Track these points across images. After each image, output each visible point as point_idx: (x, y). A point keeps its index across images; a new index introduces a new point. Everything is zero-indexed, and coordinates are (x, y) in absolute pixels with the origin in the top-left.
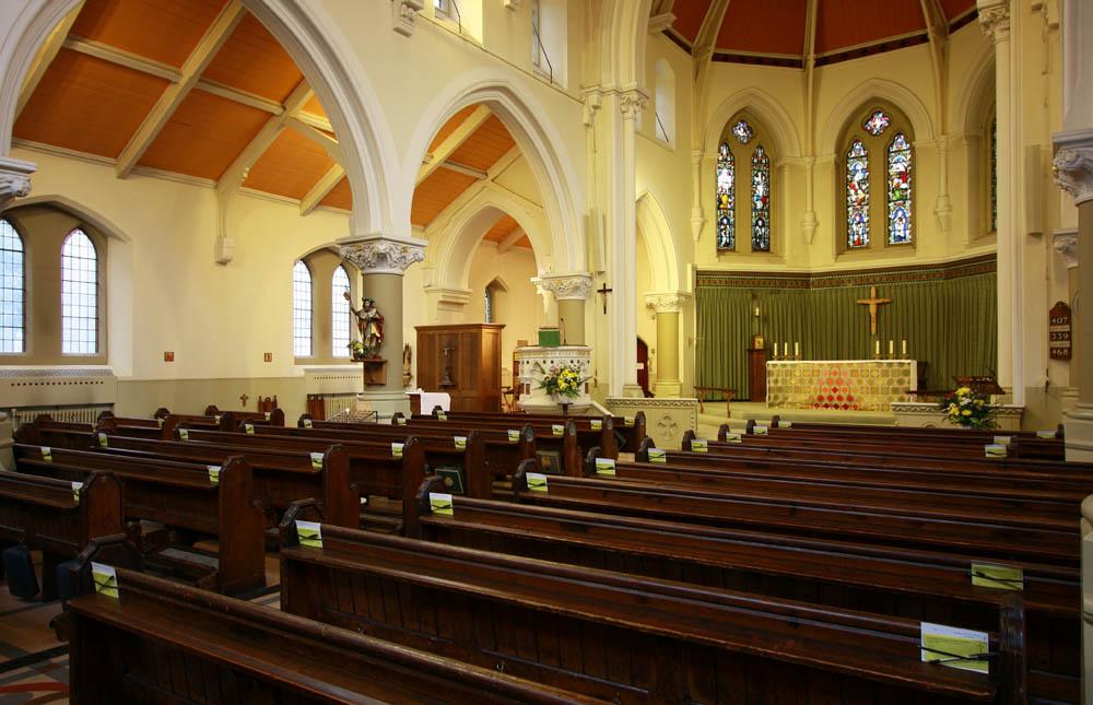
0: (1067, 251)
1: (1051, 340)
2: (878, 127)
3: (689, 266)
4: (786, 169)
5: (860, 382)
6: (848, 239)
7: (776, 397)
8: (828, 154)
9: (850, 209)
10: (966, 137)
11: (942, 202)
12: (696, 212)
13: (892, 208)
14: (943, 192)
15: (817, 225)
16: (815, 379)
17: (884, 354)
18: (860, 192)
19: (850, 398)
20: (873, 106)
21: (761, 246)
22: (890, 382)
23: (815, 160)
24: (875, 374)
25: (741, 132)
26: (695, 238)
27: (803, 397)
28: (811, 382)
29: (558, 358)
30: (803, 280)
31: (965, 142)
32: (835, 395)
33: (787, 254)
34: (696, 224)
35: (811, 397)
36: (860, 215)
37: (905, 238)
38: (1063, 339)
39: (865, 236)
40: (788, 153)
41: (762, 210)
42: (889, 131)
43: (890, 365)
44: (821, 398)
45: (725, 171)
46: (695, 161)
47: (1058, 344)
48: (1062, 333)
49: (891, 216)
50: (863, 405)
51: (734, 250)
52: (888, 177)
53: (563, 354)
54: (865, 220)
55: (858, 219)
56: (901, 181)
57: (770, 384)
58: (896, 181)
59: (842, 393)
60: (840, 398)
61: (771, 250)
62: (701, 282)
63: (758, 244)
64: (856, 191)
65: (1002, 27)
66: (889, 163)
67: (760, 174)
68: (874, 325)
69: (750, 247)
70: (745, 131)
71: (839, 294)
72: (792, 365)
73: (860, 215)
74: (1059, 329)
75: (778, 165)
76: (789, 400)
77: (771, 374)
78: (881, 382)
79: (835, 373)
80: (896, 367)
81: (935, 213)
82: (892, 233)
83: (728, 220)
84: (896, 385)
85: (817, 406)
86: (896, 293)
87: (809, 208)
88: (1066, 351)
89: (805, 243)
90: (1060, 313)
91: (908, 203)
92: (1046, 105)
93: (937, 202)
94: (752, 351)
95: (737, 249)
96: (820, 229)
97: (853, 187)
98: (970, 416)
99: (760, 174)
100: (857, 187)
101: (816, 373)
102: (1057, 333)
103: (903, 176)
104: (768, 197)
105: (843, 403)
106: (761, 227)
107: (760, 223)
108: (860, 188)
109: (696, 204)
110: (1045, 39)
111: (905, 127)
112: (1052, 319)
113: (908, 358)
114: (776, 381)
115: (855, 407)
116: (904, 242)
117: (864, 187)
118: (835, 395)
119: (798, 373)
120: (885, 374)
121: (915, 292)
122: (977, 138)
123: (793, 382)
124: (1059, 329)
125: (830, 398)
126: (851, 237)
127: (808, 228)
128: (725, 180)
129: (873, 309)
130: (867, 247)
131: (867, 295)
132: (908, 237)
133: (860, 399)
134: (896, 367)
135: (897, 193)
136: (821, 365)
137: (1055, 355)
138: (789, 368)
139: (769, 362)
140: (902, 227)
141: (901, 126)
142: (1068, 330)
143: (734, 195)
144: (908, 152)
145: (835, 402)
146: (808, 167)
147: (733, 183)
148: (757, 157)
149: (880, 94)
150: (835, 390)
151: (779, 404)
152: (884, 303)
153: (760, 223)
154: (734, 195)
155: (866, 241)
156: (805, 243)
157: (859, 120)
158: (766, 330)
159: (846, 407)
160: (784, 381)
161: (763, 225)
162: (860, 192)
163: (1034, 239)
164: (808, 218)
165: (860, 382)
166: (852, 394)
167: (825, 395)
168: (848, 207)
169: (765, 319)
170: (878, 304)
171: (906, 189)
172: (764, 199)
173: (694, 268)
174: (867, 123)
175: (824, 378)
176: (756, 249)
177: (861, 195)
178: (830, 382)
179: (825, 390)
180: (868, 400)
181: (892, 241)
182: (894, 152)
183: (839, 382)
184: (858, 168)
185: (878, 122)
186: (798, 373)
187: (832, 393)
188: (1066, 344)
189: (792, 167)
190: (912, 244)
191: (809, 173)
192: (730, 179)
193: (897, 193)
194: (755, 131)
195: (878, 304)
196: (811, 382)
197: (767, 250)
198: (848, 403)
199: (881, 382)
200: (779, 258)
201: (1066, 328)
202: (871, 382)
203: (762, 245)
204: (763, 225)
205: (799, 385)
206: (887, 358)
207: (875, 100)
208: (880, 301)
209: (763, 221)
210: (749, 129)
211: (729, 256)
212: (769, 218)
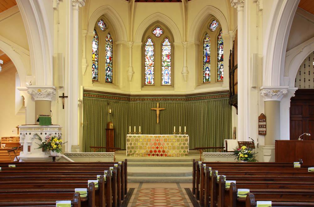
0: (266, 95)
1: (259, 128)
2: (158, 33)
3: (82, 87)
4: (121, 46)
5: (168, 144)
6: (145, 81)
7: (131, 151)
8: (138, 42)
10: (195, 44)
11: (185, 69)
12: (84, 61)
14: (185, 65)
15: (134, 73)
16: (148, 143)
17: (177, 133)
18: (150, 60)
19: (164, 151)
20: (157, 24)
21: (109, 81)
22: (180, 144)
23: (133, 44)
24: (174, 140)
25: (101, 26)
26: (83, 73)
27: (143, 151)
28: (147, 144)
29: (46, 133)
30: (127, 98)
31: (194, 46)
32: (157, 150)
33: (121, 84)
34: (84, 67)
35: (147, 151)
36: (150, 71)
37: (168, 82)
38: (263, 127)
39: (152, 80)
40: (122, 39)
41: (109, 63)
42: (163, 36)
43: (180, 137)
44: (151, 152)
45: (94, 42)
46: (84, 35)
47: (261, 129)
48: (263, 125)
49: (163, 73)
50: (169, 154)
51: (97, 81)
52: (162, 55)
53: (51, 130)
55: (149, 72)
56: (167, 58)
57: (128, 145)
59: (160, 149)
60: (159, 151)
61: (113, 82)
62: (85, 95)
63: (107, 79)
64: (149, 60)
65: (241, 6)
67: (109, 46)
68: (158, 119)
69: (104, 80)
70: (103, 25)
71: (143, 105)
72: (138, 136)
73: (150, 71)
74: (262, 123)
75: (117, 43)
76: (137, 152)
77: (128, 140)
78: (176, 144)
79: (157, 140)
80: (182, 138)
81: (182, 74)
82: (163, 80)
83: (95, 66)
84: (182, 145)
85: (149, 155)
86: (166, 106)
87: (130, 65)
88: (264, 132)
89: (128, 81)
90: (262, 118)
91: (170, 68)
92: (257, 39)
93: (183, 69)
94: (108, 129)
95: (99, 81)
96: (135, 75)
97: (148, 58)
98: (247, 157)
99: (109, 46)
100: (149, 58)
101: (149, 140)
102: (261, 125)
103: (168, 56)
104: (112, 57)
105: (161, 154)
106: (109, 71)
107: (108, 69)
109: (84, 56)
110: (257, 15)
111: (170, 36)
112: (259, 120)
113: (187, 134)
114: (131, 144)
115: (166, 155)
116: (168, 84)
118: (157, 150)
119: (141, 140)
120: (178, 140)
121: (174, 106)
122: (198, 45)
123: (139, 144)
124: (262, 123)
125: (155, 151)
126: (146, 80)
127: (130, 74)
128: (95, 47)
129: (158, 112)
130: (154, 85)
131: (155, 106)
132: (170, 82)
133: (168, 152)
134: (182, 138)
135: (165, 63)
136: (151, 136)
137: (260, 133)
138: (137, 138)
139: (127, 135)
140: (167, 78)
141: (168, 34)
142: (265, 124)
143: (98, 55)
145: (157, 153)
146: (130, 46)
147: (98, 49)
148: (108, 38)
149: (161, 20)
150: (157, 148)
151: (132, 155)
152: (161, 110)
153: (108, 69)
154: (98, 55)
155: (153, 82)
156: (128, 81)
157: (152, 28)
158: (113, 120)
159: (162, 155)
160: (135, 144)
161: (110, 71)
162: (150, 60)
163: (253, 89)
164: (130, 69)
165: (168, 144)
166: (165, 149)
167: (153, 150)
168: (145, 66)
169: (112, 114)
170: (160, 110)
171: (169, 62)
172: (110, 58)
173: (83, 88)
175: (153, 142)
176: (107, 82)
177: (151, 62)
178: (155, 144)
179: (153, 148)
180: (171, 152)
181: (163, 84)
183: (159, 144)
184: (149, 50)
185: (158, 32)
186: (141, 140)
187: (156, 149)
188: (264, 129)
189: (124, 45)
190: (172, 85)
191: (130, 49)
192: (96, 47)
193: (165, 63)
194: (107, 27)
195: (160, 110)
196: (147, 144)
197: (111, 82)
198: (163, 154)
199: (176, 144)
200: (117, 87)
201: (264, 123)
202: (172, 144)
203: (109, 80)
204: (110, 71)
205: (141, 146)
206: (178, 134)
207: (158, 22)
208: (161, 109)
209: (110, 69)
210: (104, 24)
211: (96, 83)
212: (112, 67)
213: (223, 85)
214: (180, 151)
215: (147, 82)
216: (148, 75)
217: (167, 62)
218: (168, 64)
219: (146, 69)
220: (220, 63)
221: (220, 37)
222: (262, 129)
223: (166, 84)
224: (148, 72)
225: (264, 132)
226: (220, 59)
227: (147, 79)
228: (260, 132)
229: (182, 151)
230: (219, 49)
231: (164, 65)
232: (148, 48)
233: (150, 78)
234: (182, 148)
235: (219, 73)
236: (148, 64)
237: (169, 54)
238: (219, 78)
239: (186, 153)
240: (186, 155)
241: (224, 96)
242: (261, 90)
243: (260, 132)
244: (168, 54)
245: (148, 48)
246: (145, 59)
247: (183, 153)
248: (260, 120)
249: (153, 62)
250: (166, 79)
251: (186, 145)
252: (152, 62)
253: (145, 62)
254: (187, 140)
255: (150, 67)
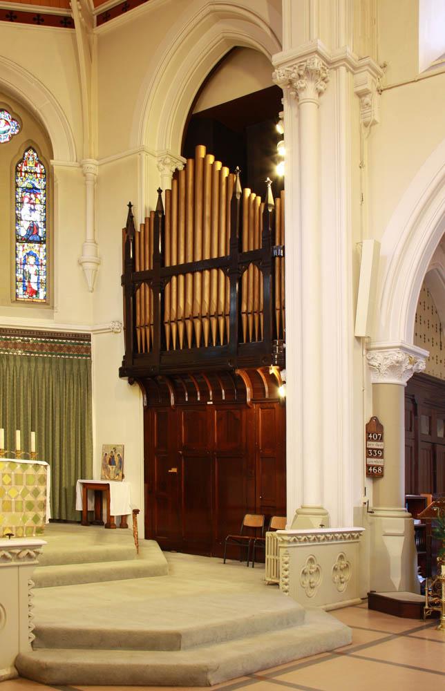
22: (25, 492)
38: (378, 457)
47: (373, 461)
48: (378, 450)
74: (374, 445)
84: (29, 498)
90: (374, 429)
102: (373, 449)
112: (368, 433)
120: (18, 480)
124: (374, 445)
134: (30, 471)
142: (369, 443)
199: (13, 493)
213: (55, 314)
214: (25, 518)
220: (26, 247)
221: (24, 169)
222: (375, 460)
225: (380, 470)
226: (23, 232)
228: (370, 469)
229: (31, 514)
230: (22, 203)
234: (30, 506)
235: (20, 276)
238: (20, 291)
239: (40, 524)
240: (40, 531)
241: (60, 348)
242: (368, 350)
243: (370, 469)
247: (33, 524)
248: (370, 436)
251: (41, 498)
254: (42, 480)
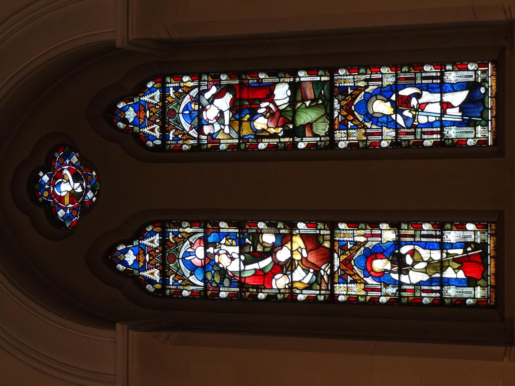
9: (340, 289)
13: (356, 135)
18: (283, 255)
54: (389, 236)
58: (260, 123)
66: (197, 148)
82: (452, 132)
100: (266, 263)
108: (272, 251)
117: (269, 239)
126: (452, 292)
144: (171, 85)
162: (283, 255)
168: (333, 297)
171: (295, 87)
174: (59, 224)
182: (164, 131)
215: (471, 282)
216: (404, 279)
217: (293, 101)
218: (310, 94)
219: (356, 290)
223: (490, 103)
224: (381, 276)
227: (443, 282)
231: (322, 128)
232: (187, 273)
233: (436, 255)
236: (309, 278)
237: (228, 89)
244: (228, 97)
245: (187, 273)
246: (269, 297)
249: (294, 226)
250: (445, 106)
252: (298, 242)
253: (293, 296)
255: (337, 263)
